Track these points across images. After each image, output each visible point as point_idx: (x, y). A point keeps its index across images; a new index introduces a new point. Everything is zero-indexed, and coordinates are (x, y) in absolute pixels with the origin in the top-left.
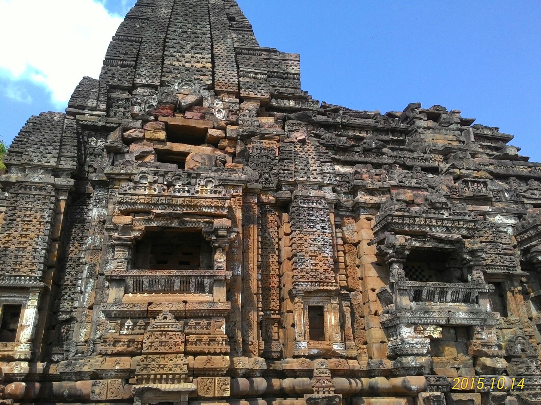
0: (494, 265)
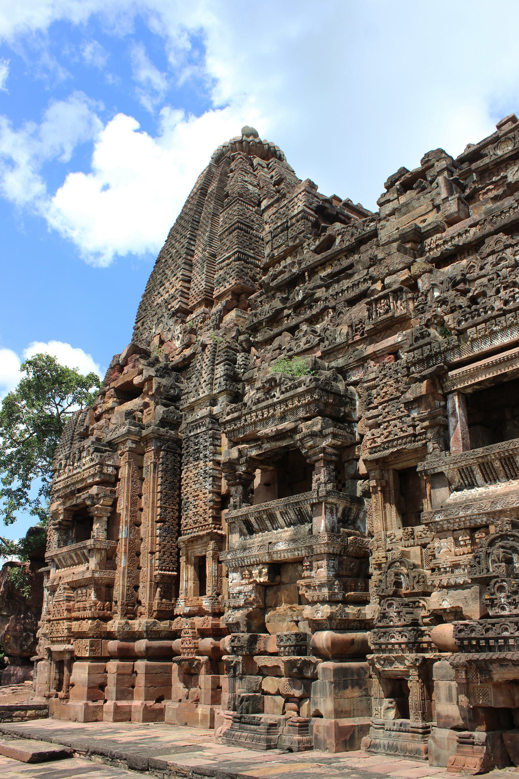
0: (389, 442)
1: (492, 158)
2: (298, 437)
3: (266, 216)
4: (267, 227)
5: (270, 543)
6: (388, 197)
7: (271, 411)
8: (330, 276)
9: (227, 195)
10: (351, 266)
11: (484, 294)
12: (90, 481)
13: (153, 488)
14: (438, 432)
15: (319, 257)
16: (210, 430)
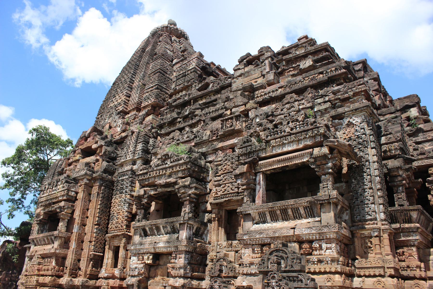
0: (224, 195)
1: (294, 55)
2: (177, 187)
3: (175, 68)
4: (175, 74)
5: (155, 242)
6: (239, 67)
7: (164, 172)
8: (204, 104)
9: (156, 54)
10: (216, 100)
11: (281, 123)
12: (60, 198)
13: (96, 206)
14: (250, 192)
15: (200, 93)
16: (131, 178)
